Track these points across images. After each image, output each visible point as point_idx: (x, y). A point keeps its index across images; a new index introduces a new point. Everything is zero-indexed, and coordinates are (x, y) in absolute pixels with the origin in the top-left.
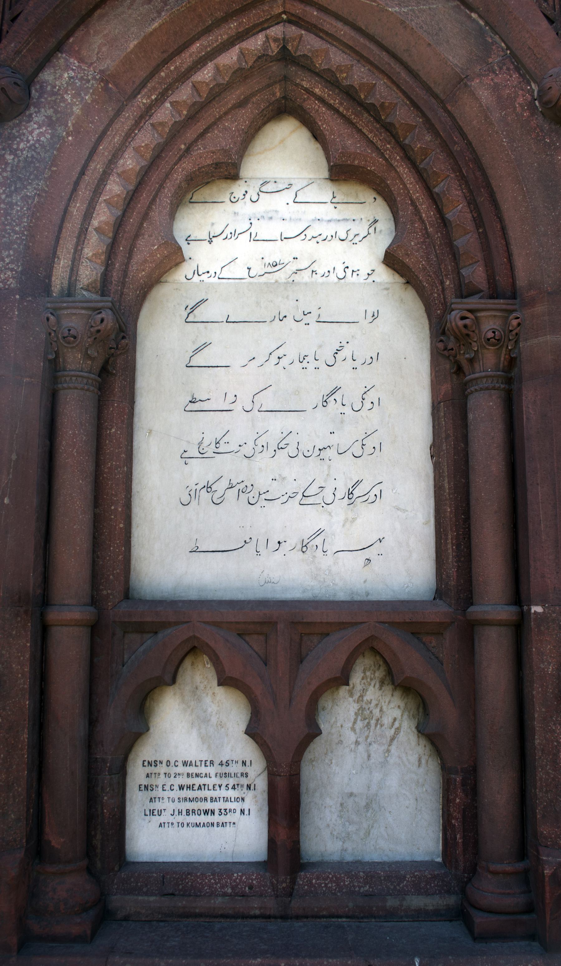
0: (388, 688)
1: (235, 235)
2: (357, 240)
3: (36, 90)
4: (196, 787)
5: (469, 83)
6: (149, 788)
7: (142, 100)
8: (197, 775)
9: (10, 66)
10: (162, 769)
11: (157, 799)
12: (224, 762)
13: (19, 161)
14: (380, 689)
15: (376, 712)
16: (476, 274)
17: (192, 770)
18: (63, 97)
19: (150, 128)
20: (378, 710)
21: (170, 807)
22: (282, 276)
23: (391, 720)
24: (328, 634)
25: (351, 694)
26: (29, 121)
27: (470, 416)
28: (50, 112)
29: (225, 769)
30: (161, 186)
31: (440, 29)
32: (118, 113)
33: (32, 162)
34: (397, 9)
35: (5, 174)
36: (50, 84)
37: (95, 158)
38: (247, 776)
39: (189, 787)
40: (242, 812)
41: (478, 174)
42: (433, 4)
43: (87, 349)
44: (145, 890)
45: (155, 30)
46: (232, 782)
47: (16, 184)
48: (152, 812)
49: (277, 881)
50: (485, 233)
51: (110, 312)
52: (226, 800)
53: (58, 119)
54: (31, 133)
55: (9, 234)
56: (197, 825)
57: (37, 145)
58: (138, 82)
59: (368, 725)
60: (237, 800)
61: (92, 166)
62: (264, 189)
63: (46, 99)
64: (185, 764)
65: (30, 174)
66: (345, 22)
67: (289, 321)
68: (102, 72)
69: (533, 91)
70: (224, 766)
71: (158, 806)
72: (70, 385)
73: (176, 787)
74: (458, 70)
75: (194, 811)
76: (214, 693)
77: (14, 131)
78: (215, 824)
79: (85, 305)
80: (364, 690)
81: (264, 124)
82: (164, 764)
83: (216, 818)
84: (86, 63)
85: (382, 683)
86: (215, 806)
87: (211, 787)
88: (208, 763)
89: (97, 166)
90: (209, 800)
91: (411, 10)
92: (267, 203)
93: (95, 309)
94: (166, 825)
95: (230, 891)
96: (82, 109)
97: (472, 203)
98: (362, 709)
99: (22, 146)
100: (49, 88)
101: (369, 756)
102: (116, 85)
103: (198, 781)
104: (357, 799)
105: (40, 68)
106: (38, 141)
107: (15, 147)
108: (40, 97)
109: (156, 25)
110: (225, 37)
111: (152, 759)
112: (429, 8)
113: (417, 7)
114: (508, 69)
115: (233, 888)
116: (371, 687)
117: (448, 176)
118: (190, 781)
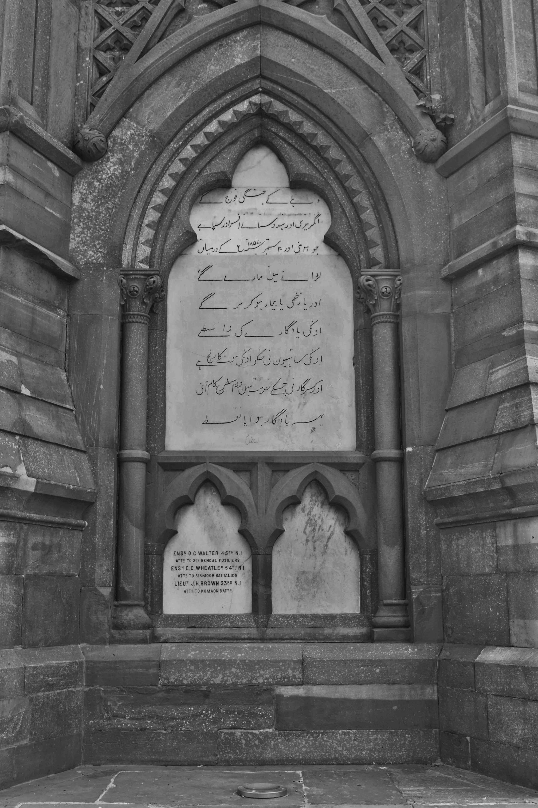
0: (326, 507)
1: (229, 224)
3: (111, 142)
4: (207, 568)
5: (372, 138)
6: (178, 569)
7: (173, 145)
8: (208, 561)
9: (97, 129)
10: (186, 557)
11: (183, 576)
12: (224, 553)
13: (103, 186)
14: (322, 507)
15: (319, 522)
16: (378, 253)
17: (204, 557)
18: (127, 147)
19: (178, 162)
20: (320, 520)
21: (191, 580)
22: (259, 251)
24: (288, 471)
25: (303, 511)
26: (108, 161)
27: (374, 338)
28: (120, 156)
29: (224, 557)
30: (184, 196)
31: (356, 103)
33: (110, 187)
34: (329, 90)
36: (120, 138)
37: (146, 182)
38: (239, 561)
39: (202, 568)
41: (379, 192)
42: (351, 87)
43: (143, 299)
44: (177, 624)
45: (182, 104)
46: (229, 564)
47: (101, 200)
48: (180, 584)
49: (258, 618)
50: (383, 227)
51: (158, 277)
52: (226, 575)
53: (125, 160)
54: (109, 169)
55: (98, 230)
56: (208, 591)
57: (113, 177)
58: (171, 134)
59: (314, 530)
60: (232, 575)
61: (144, 187)
62: (247, 194)
63: (117, 148)
64: (200, 553)
65: (110, 195)
66: (298, 95)
67: (264, 280)
68: (151, 131)
69: (411, 142)
70: (224, 555)
71: (183, 579)
72: (134, 320)
73: (195, 568)
74: (366, 129)
75: (205, 583)
76: (218, 510)
77: (99, 167)
78: (219, 591)
79: (143, 272)
80: (312, 508)
81: (247, 151)
82: (187, 553)
83: (220, 587)
84: (141, 125)
85: (323, 504)
86: (219, 579)
87: (216, 568)
88: (215, 553)
89: (147, 187)
90: (215, 575)
91: (338, 91)
92: (249, 204)
93: (148, 275)
94: (189, 591)
95: (229, 624)
96: (139, 154)
97: (375, 208)
98: (310, 519)
99: (104, 176)
100: (119, 141)
101: (315, 548)
102: (159, 138)
103: (208, 564)
104: (307, 575)
105: (114, 128)
106: (114, 174)
107: (100, 177)
108: (113, 146)
109: (183, 101)
110: (224, 104)
112: (349, 90)
113: (342, 89)
114: (396, 128)
115: (231, 623)
116: (316, 506)
117: (361, 192)
118: (203, 564)
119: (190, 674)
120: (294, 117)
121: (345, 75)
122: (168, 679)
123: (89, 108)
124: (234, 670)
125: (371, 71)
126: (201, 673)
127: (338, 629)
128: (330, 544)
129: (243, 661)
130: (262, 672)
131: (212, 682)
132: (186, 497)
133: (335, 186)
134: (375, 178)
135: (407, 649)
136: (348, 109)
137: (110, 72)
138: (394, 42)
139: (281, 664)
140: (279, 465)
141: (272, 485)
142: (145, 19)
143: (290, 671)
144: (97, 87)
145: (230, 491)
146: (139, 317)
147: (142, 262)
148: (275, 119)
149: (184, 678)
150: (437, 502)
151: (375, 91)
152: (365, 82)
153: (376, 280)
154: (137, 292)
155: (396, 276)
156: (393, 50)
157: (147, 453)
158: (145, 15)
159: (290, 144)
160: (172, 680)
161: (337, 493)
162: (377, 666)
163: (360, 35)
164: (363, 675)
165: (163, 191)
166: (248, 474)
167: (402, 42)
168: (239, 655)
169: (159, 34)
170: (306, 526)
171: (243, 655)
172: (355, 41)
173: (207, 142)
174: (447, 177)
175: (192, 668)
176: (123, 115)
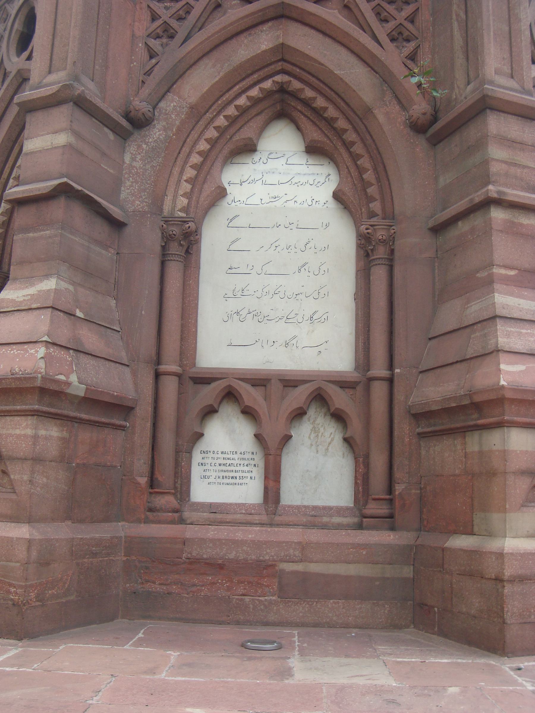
0: (328, 417)
1: (254, 181)
2: (320, 184)
4: (227, 465)
7: (209, 115)
8: (228, 459)
10: (211, 455)
16: (376, 206)
19: (213, 129)
20: (323, 428)
21: (214, 474)
22: (279, 203)
23: (329, 434)
24: (297, 387)
25: (309, 421)
27: (371, 278)
28: (164, 123)
32: (197, 122)
34: (339, 72)
35: (142, 154)
40: (251, 478)
41: (378, 156)
44: (201, 510)
45: (217, 82)
46: (246, 462)
48: (205, 477)
49: (268, 506)
50: (381, 185)
51: (193, 223)
52: (243, 471)
54: (155, 134)
58: (207, 107)
59: (318, 435)
60: (248, 472)
61: (184, 149)
64: (222, 453)
66: (313, 76)
67: (282, 227)
71: (207, 474)
72: (172, 258)
73: (217, 465)
75: (226, 477)
80: (316, 419)
82: (212, 452)
83: (237, 481)
85: (325, 415)
87: (235, 465)
88: (234, 453)
89: (186, 149)
92: (272, 164)
93: (185, 222)
97: (375, 169)
98: (314, 427)
99: (150, 140)
100: (164, 111)
101: (317, 451)
103: (229, 462)
105: (160, 101)
106: (159, 138)
107: (147, 141)
109: (217, 79)
110: (252, 82)
111: (205, 450)
116: (320, 416)
117: (364, 156)
118: (225, 462)
119: (209, 550)
120: (309, 93)
121: (353, 60)
122: (191, 554)
123: (140, 85)
124: (245, 548)
125: (374, 56)
126: (218, 549)
127: (334, 518)
128: (330, 448)
129: (253, 541)
130: (268, 551)
131: (227, 557)
132: (211, 406)
133: (343, 150)
134: (376, 145)
135: (389, 536)
136: (354, 88)
137: (158, 55)
138: (394, 33)
139: (284, 544)
140: (290, 382)
141: (283, 398)
142: (188, 13)
143: (291, 551)
144: (148, 68)
145: (248, 402)
146: (176, 256)
147: (180, 210)
148: (294, 95)
149: (204, 553)
150: (419, 416)
151: (377, 73)
152: (369, 65)
153: (374, 229)
154: (175, 235)
155: (391, 226)
156: (393, 40)
157: (180, 368)
158: (188, 9)
159: (305, 116)
160: (194, 554)
161: (337, 406)
162: (363, 549)
163: (365, 27)
164: (352, 556)
165: (200, 153)
166: (263, 388)
167: (400, 33)
168: (250, 536)
169: (199, 25)
170: (311, 433)
171: (253, 536)
172: (361, 31)
173: (236, 113)
174: (435, 145)
175: (211, 545)
176: (168, 91)
